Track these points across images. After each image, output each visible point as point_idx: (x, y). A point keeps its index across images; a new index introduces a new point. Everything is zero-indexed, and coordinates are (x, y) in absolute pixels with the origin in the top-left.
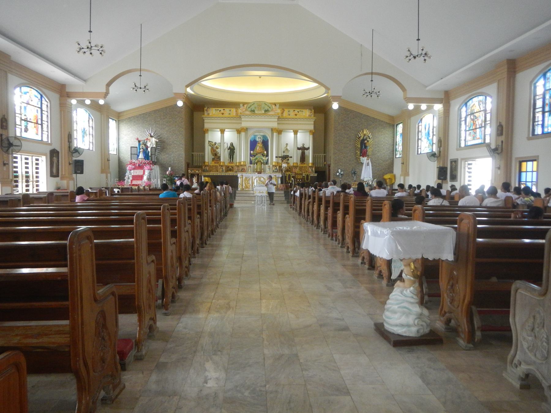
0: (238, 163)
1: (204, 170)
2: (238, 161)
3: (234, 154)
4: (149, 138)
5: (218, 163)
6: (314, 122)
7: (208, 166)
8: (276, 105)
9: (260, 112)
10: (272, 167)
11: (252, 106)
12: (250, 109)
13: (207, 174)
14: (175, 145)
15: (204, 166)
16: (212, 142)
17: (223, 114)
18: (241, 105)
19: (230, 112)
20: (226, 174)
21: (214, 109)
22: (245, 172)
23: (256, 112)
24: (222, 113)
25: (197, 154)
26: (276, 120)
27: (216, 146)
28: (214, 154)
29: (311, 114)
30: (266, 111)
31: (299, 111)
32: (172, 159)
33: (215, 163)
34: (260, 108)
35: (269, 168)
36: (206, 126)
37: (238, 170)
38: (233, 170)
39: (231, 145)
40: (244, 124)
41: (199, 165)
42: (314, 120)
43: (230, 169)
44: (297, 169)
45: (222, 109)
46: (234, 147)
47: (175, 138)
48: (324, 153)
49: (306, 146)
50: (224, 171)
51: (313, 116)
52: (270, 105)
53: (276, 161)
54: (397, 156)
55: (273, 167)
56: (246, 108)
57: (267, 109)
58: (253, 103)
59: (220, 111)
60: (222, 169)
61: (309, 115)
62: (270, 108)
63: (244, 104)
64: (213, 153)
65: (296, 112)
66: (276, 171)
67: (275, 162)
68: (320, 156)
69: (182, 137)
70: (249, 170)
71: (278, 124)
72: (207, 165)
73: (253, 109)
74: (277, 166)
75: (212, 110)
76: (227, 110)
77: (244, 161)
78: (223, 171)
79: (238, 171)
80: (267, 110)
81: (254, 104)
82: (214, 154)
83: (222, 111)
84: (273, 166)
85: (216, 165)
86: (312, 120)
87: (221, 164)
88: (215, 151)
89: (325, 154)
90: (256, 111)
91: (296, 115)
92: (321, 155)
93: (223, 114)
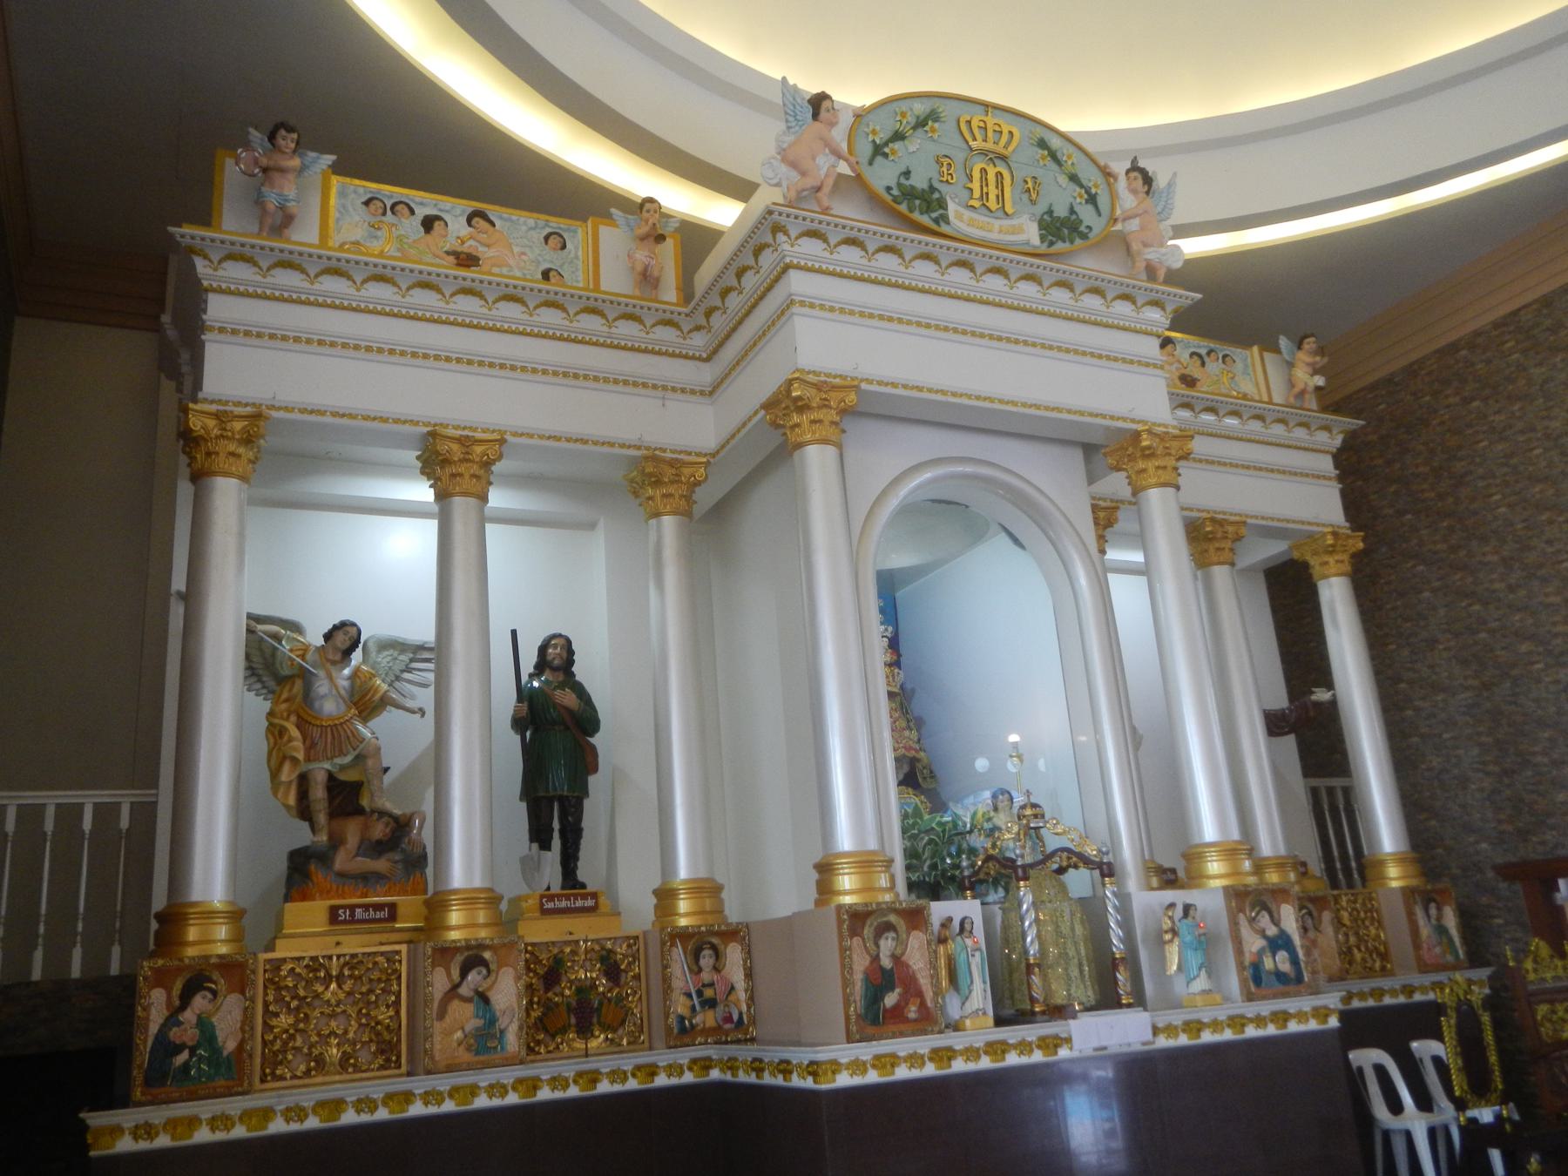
0: (683, 905)
1: (165, 1047)
3: (586, 794)
5: (392, 912)
6: (1339, 457)
7: (234, 971)
9: (994, 229)
10: (1234, 924)
11: (914, 143)
12: (883, 176)
13: (214, 1123)
15: (161, 979)
16: (295, 627)
19: (550, 258)
20: (533, 1085)
23: (959, 217)
24: (451, 243)
27: (356, 673)
28: (320, 778)
30: (1058, 228)
31: (1203, 352)
33: (333, 911)
34: (999, 175)
37: (711, 1004)
38: (620, 999)
39: (542, 665)
42: (1338, 441)
43: (584, 990)
45: (454, 211)
50: (513, 1041)
52: (1090, 176)
53: (1235, 835)
55: (1242, 918)
57: (1061, 211)
58: (920, 108)
59: (428, 223)
60: (483, 998)
62: (1092, 199)
64: (303, 781)
66: (1280, 976)
67: (1229, 852)
73: (919, 181)
77: (872, 845)
78: (485, 1041)
80: (1064, 222)
81: (933, 116)
82: (319, 793)
85: (354, 944)
86: (1322, 437)
87: (458, 924)
88: (338, 736)
90: (952, 208)
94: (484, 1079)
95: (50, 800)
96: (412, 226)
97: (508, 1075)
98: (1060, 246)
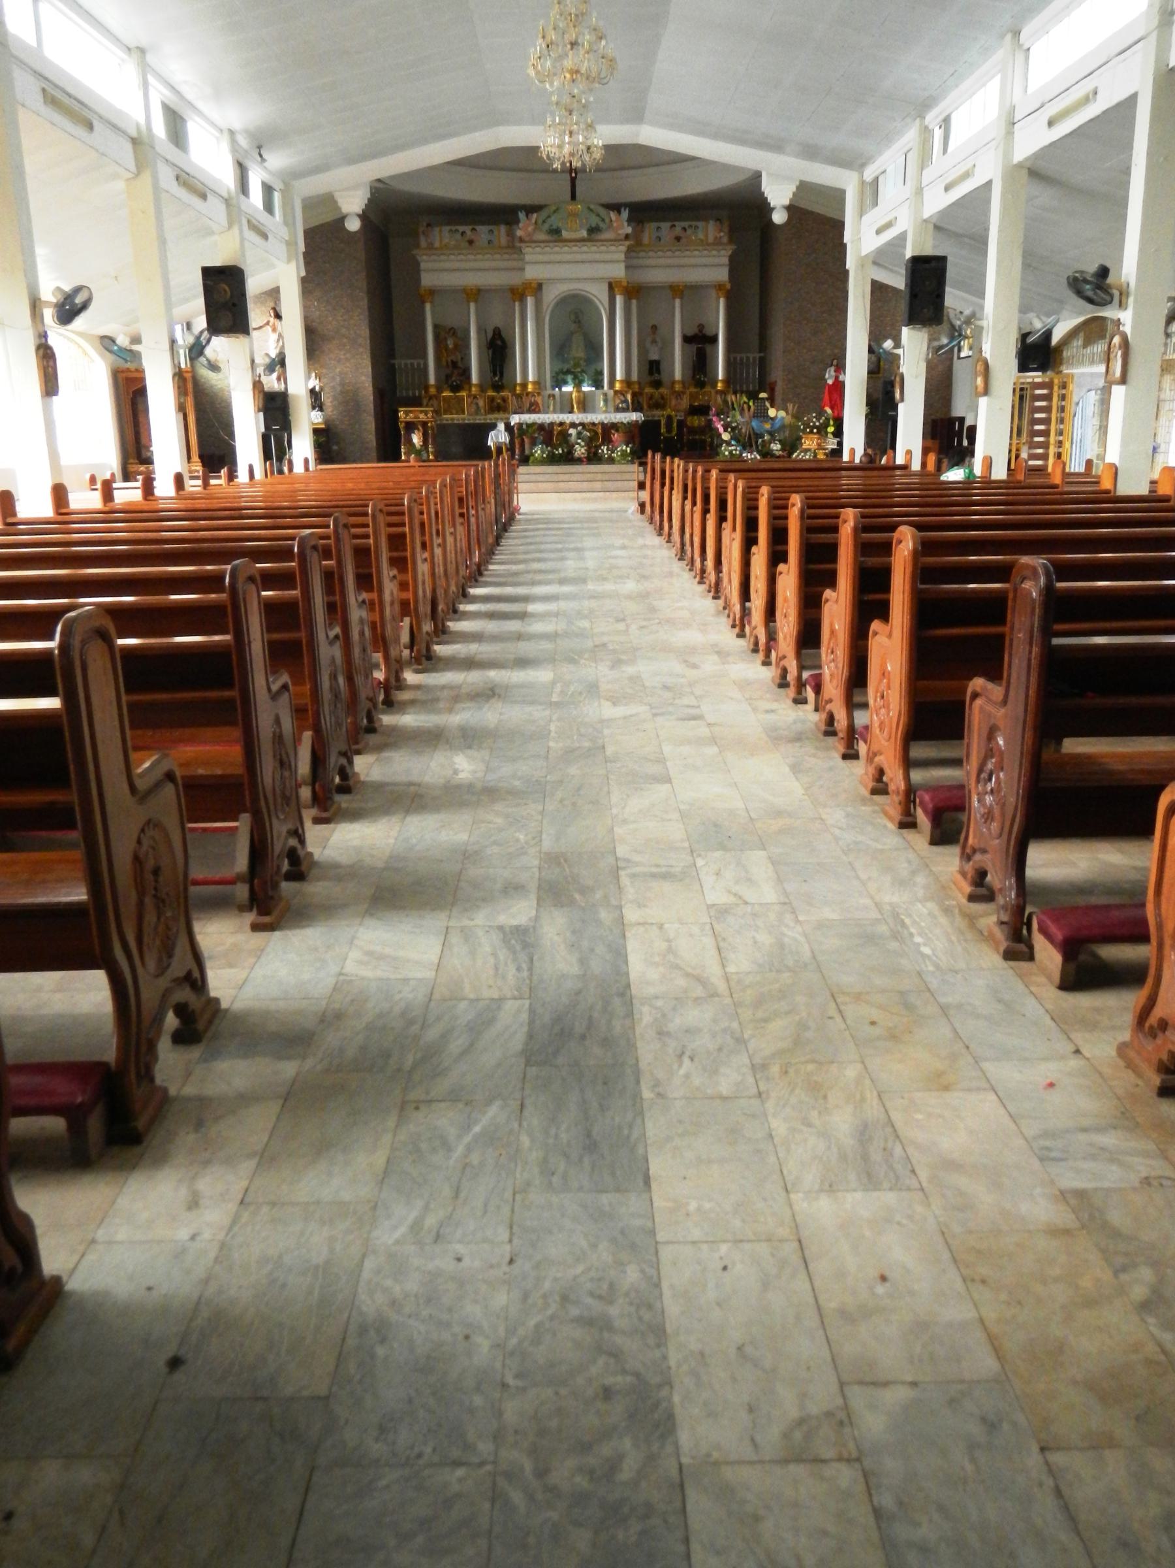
2: (519, 380)
4: (272, 320)
6: (733, 260)
8: (619, 212)
11: (553, 218)
12: (546, 226)
14: (345, 340)
17: (471, 242)
18: (522, 215)
21: (446, 228)
22: (539, 412)
23: (565, 234)
25: (406, 365)
26: (622, 256)
29: (722, 234)
30: (593, 230)
32: (338, 379)
35: (606, 401)
36: (428, 280)
40: (532, 273)
41: (411, 394)
42: (730, 252)
43: (498, 404)
44: (682, 399)
45: (467, 229)
46: (503, 341)
47: (345, 320)
48: (760, 352)
49: (709, 332)
51: (725, 240)
54: (963, 355)
56: (536, 223)
57: (594, 225)
58: (554, 208)
60: (477, 404)
61: (716, 238)
62: (603, 220)
63: (531, 209)
65: (678, 230)
67: (621, 381)
68: (748, 358)
69: (362, 317)
70: (549, 407)
71: (627, 267)
72: (435, 396)
73: (554, 227)
74: (627, 392)
75: (441, 231)
76: (483, 229)
79: (520, 410)
81: (557, 209)
82: (450, 364)
83: (469, 233)
84: (616, 392)
86: (723, 252)
89: (762, 355)
91: (678, 239)
92: (751, 356)
93: (471, 242)
94: (478, 417)
95: (409, 362)
96: (458, 236)
97: (482, 417)
98: (593, 236)
